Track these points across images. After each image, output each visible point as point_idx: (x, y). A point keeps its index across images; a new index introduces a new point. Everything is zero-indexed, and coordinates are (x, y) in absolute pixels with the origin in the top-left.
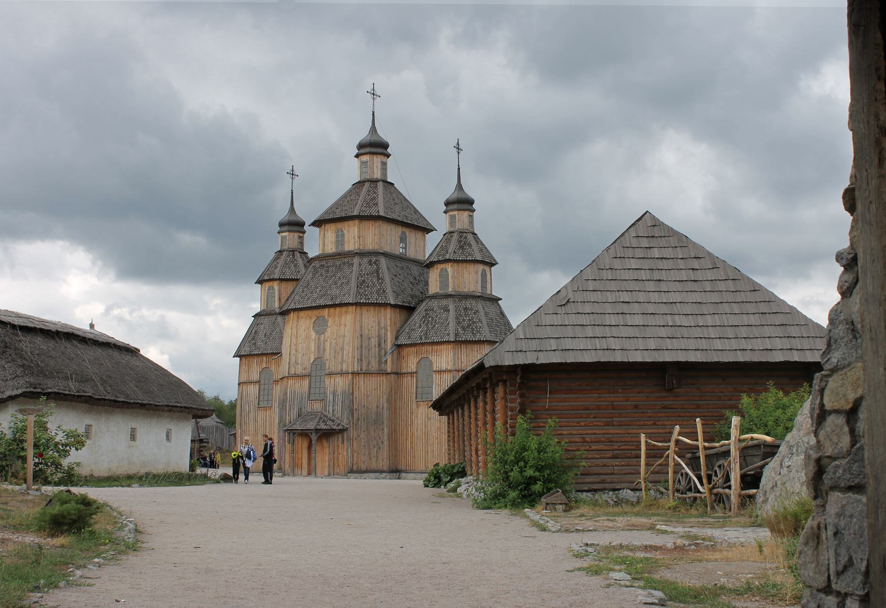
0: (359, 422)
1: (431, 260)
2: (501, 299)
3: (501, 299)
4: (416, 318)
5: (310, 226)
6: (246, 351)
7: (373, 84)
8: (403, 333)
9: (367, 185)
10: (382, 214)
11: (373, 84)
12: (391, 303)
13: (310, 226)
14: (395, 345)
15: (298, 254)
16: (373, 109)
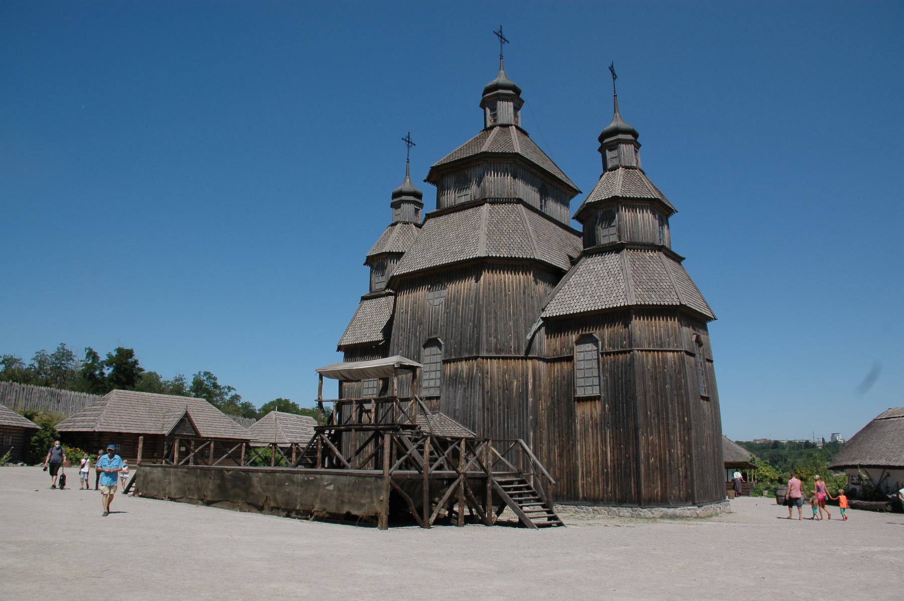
0: (493, 428)
1: (590, 201)
2: (684, 259)
3: (684, 259)
4: (570, 280)
5: (425, 181)
6: (349, 340)
7: (501, 26)
8: (554, 301)
9: (497, 129)
10: (518, 149)
11: (501, 26)
12: (536, 258)
13: (425, 181)
14: (541, 317)
15: (414, 226)
16: (502, 53)
